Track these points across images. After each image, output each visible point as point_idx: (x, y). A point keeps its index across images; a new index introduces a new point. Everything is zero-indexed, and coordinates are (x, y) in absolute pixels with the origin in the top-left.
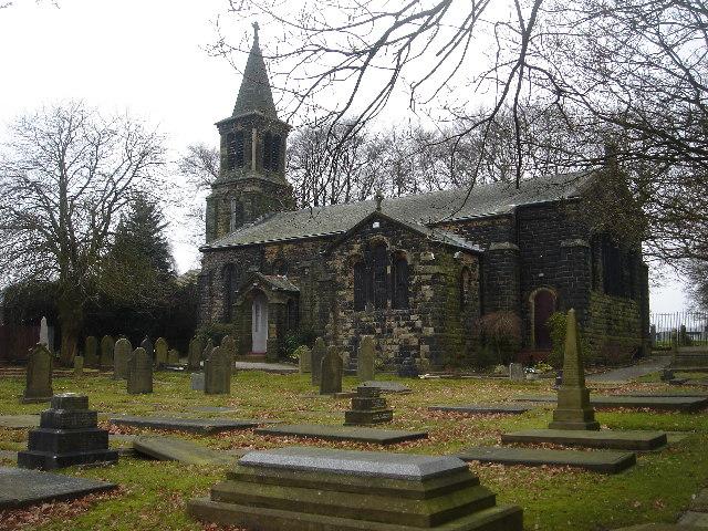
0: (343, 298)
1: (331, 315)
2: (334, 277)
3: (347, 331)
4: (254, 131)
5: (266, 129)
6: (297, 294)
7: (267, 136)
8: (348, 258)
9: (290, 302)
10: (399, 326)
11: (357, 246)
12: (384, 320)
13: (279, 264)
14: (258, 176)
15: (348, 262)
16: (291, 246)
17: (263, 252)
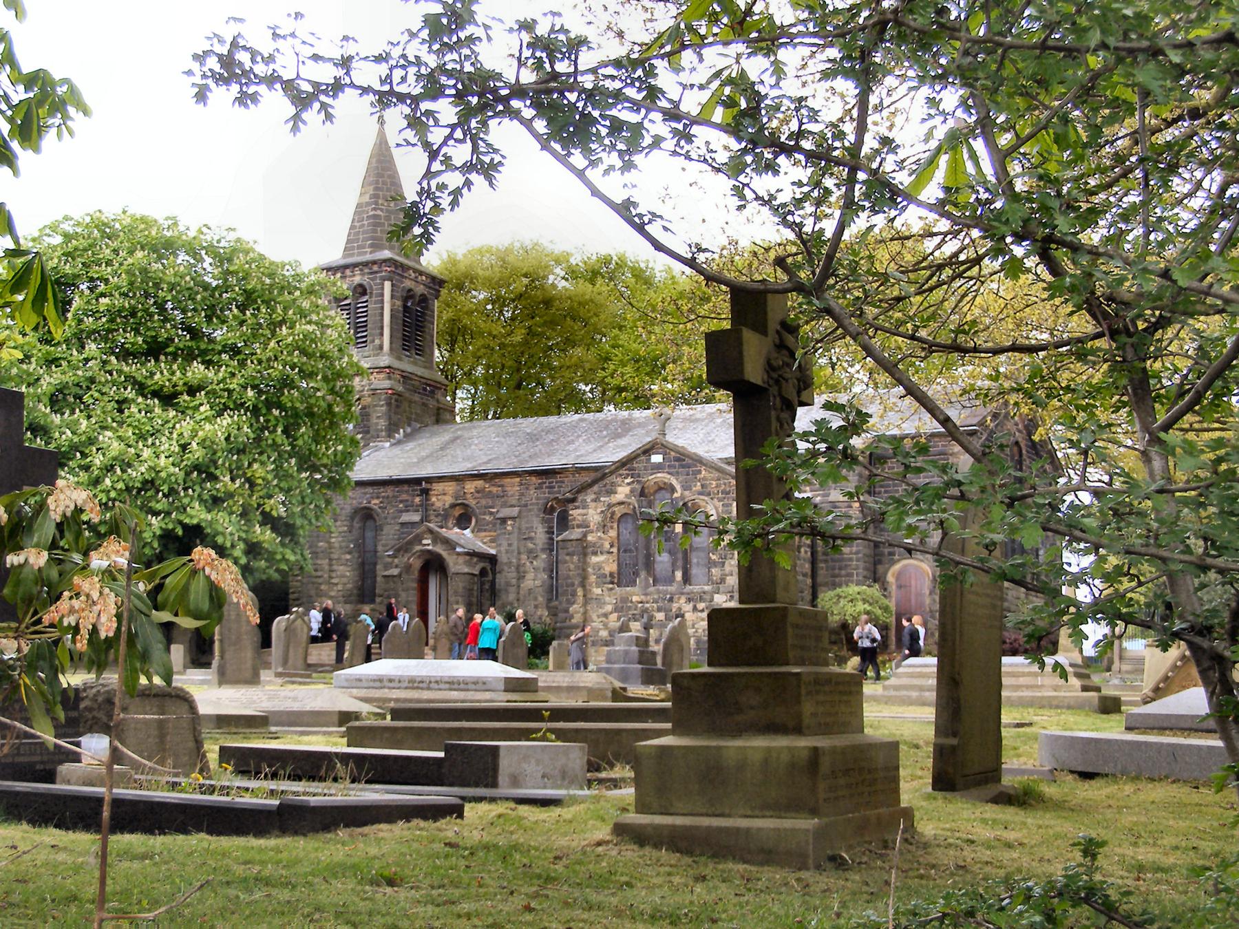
0: (599, 567)
1: (580, 592)
2: (585, 535)
3: (606, 615)
4: (387, 285)
5: (408, 284)
6: (492, 560)
7: (409, 294)
8: (610, 506)
9: (483, 572)
10: (695, 609)
11: (627, 490)
12: (671, 600)
13: (457, 512)
14: (396, 364)
15: (609, 517)
16: (479, 483)
17: (426, 492)
